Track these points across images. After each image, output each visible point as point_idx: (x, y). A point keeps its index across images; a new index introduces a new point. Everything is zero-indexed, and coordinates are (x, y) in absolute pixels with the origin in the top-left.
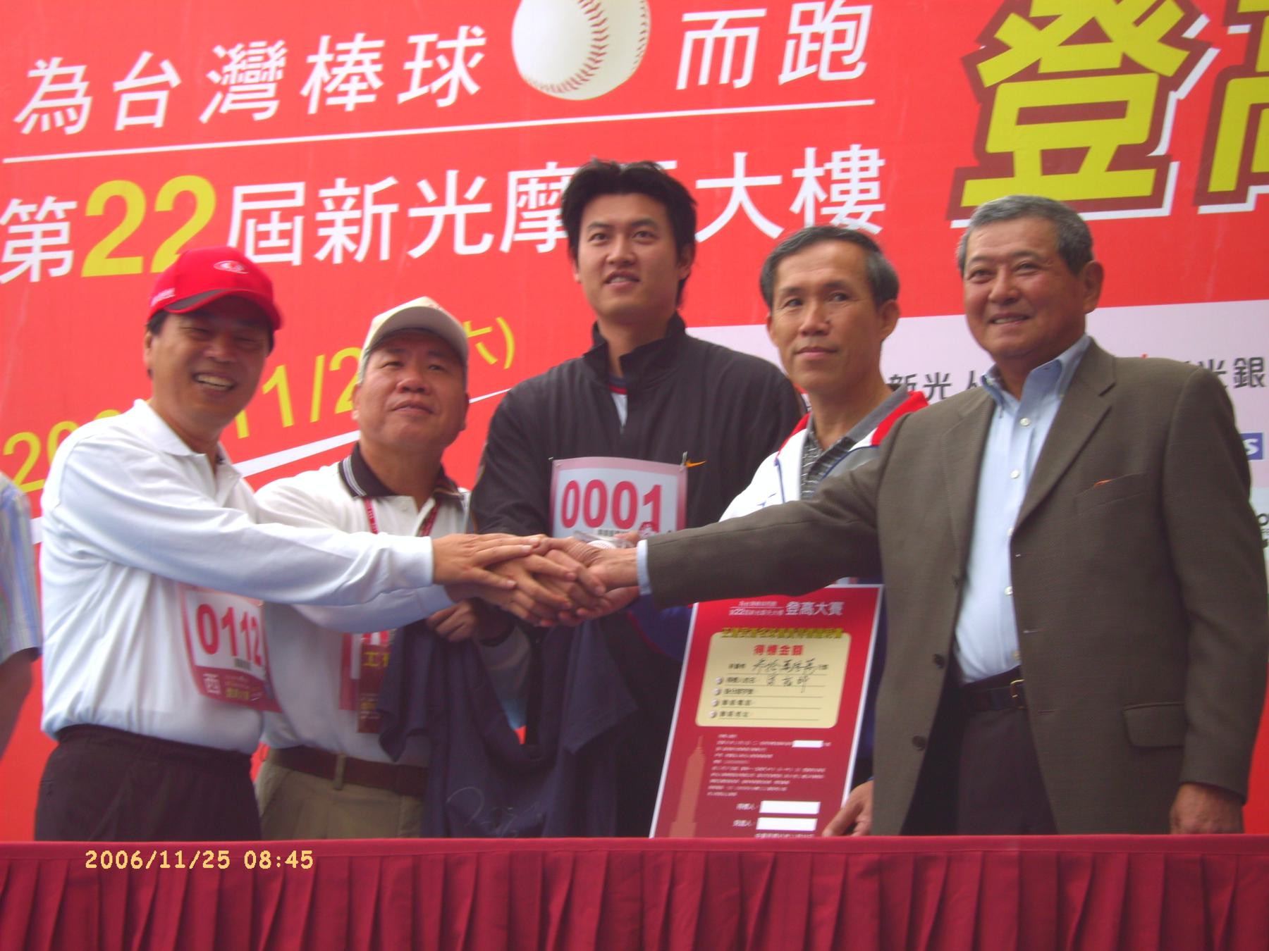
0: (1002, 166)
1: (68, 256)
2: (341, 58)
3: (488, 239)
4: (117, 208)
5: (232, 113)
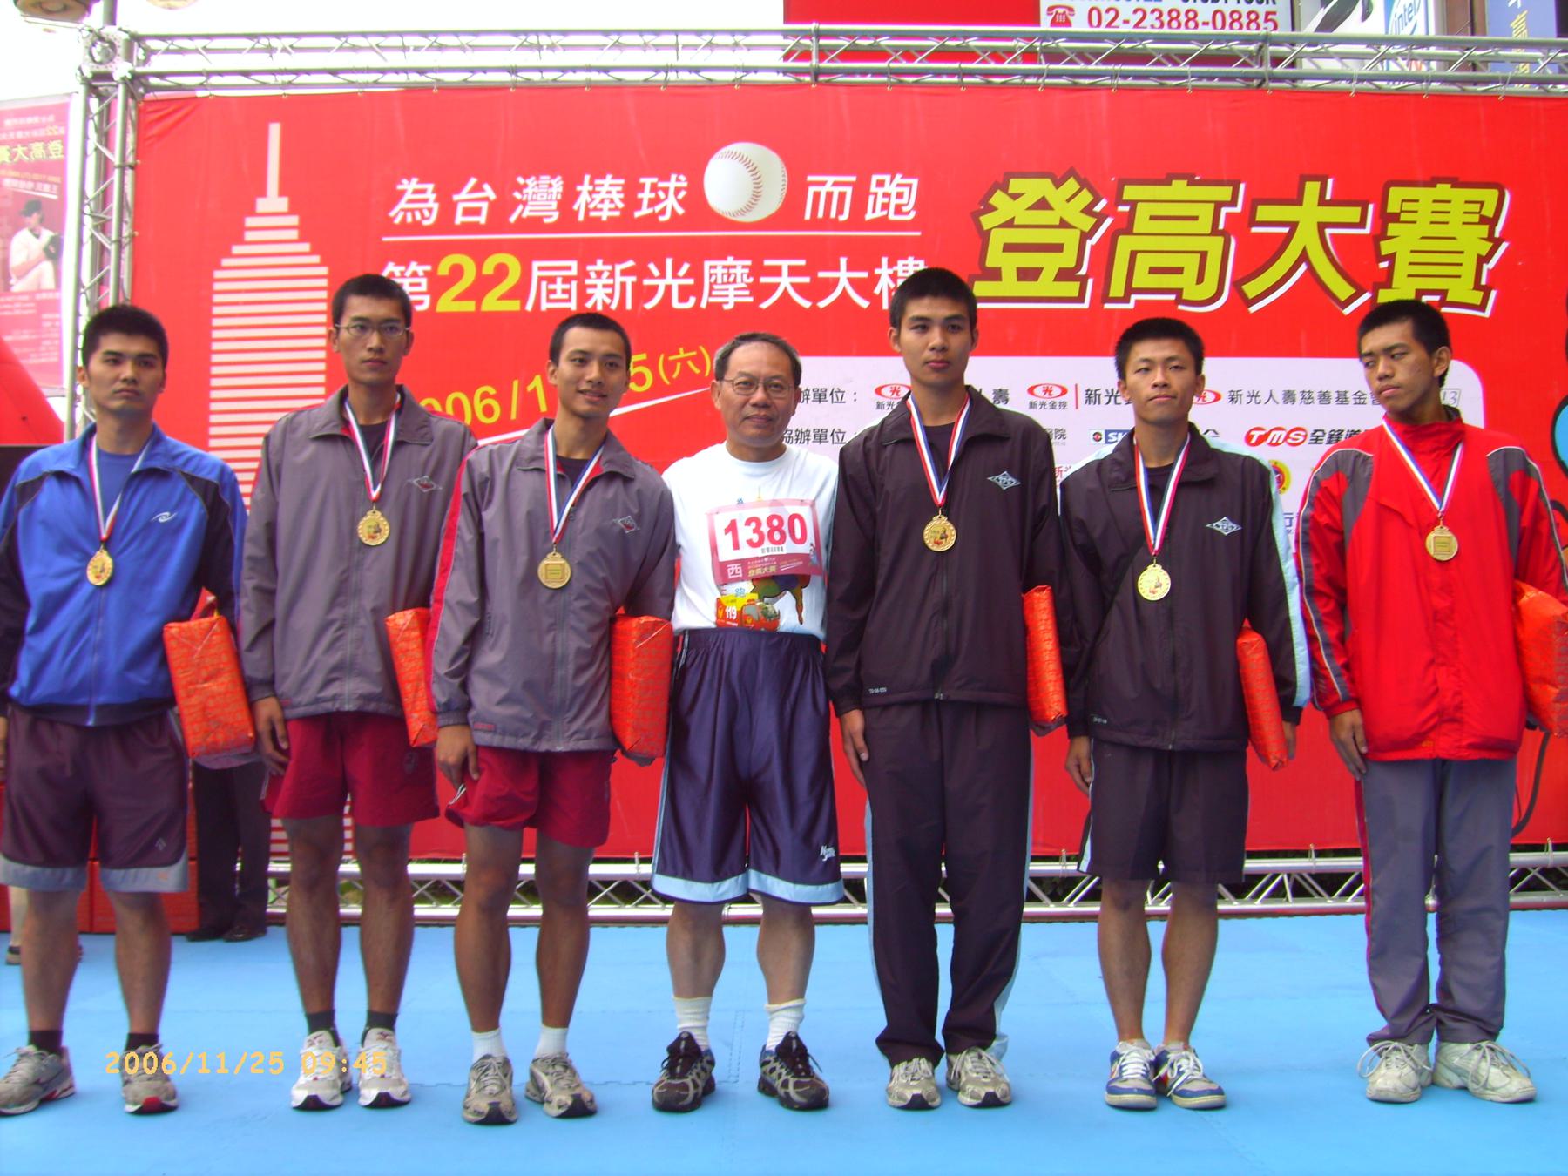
0: (995, 275)
1: (427, 299)
2: (597, 189)
3: (692, 301)
4: (457, 272)
5: (530, 219)
